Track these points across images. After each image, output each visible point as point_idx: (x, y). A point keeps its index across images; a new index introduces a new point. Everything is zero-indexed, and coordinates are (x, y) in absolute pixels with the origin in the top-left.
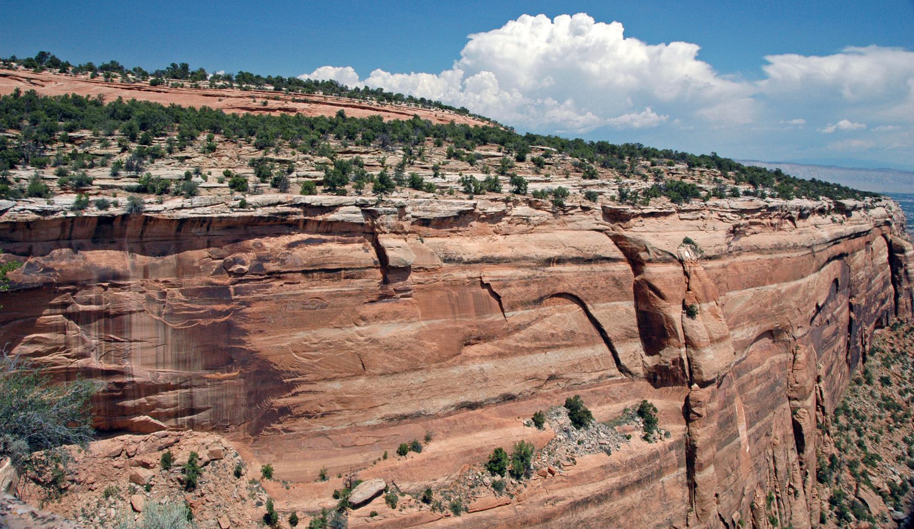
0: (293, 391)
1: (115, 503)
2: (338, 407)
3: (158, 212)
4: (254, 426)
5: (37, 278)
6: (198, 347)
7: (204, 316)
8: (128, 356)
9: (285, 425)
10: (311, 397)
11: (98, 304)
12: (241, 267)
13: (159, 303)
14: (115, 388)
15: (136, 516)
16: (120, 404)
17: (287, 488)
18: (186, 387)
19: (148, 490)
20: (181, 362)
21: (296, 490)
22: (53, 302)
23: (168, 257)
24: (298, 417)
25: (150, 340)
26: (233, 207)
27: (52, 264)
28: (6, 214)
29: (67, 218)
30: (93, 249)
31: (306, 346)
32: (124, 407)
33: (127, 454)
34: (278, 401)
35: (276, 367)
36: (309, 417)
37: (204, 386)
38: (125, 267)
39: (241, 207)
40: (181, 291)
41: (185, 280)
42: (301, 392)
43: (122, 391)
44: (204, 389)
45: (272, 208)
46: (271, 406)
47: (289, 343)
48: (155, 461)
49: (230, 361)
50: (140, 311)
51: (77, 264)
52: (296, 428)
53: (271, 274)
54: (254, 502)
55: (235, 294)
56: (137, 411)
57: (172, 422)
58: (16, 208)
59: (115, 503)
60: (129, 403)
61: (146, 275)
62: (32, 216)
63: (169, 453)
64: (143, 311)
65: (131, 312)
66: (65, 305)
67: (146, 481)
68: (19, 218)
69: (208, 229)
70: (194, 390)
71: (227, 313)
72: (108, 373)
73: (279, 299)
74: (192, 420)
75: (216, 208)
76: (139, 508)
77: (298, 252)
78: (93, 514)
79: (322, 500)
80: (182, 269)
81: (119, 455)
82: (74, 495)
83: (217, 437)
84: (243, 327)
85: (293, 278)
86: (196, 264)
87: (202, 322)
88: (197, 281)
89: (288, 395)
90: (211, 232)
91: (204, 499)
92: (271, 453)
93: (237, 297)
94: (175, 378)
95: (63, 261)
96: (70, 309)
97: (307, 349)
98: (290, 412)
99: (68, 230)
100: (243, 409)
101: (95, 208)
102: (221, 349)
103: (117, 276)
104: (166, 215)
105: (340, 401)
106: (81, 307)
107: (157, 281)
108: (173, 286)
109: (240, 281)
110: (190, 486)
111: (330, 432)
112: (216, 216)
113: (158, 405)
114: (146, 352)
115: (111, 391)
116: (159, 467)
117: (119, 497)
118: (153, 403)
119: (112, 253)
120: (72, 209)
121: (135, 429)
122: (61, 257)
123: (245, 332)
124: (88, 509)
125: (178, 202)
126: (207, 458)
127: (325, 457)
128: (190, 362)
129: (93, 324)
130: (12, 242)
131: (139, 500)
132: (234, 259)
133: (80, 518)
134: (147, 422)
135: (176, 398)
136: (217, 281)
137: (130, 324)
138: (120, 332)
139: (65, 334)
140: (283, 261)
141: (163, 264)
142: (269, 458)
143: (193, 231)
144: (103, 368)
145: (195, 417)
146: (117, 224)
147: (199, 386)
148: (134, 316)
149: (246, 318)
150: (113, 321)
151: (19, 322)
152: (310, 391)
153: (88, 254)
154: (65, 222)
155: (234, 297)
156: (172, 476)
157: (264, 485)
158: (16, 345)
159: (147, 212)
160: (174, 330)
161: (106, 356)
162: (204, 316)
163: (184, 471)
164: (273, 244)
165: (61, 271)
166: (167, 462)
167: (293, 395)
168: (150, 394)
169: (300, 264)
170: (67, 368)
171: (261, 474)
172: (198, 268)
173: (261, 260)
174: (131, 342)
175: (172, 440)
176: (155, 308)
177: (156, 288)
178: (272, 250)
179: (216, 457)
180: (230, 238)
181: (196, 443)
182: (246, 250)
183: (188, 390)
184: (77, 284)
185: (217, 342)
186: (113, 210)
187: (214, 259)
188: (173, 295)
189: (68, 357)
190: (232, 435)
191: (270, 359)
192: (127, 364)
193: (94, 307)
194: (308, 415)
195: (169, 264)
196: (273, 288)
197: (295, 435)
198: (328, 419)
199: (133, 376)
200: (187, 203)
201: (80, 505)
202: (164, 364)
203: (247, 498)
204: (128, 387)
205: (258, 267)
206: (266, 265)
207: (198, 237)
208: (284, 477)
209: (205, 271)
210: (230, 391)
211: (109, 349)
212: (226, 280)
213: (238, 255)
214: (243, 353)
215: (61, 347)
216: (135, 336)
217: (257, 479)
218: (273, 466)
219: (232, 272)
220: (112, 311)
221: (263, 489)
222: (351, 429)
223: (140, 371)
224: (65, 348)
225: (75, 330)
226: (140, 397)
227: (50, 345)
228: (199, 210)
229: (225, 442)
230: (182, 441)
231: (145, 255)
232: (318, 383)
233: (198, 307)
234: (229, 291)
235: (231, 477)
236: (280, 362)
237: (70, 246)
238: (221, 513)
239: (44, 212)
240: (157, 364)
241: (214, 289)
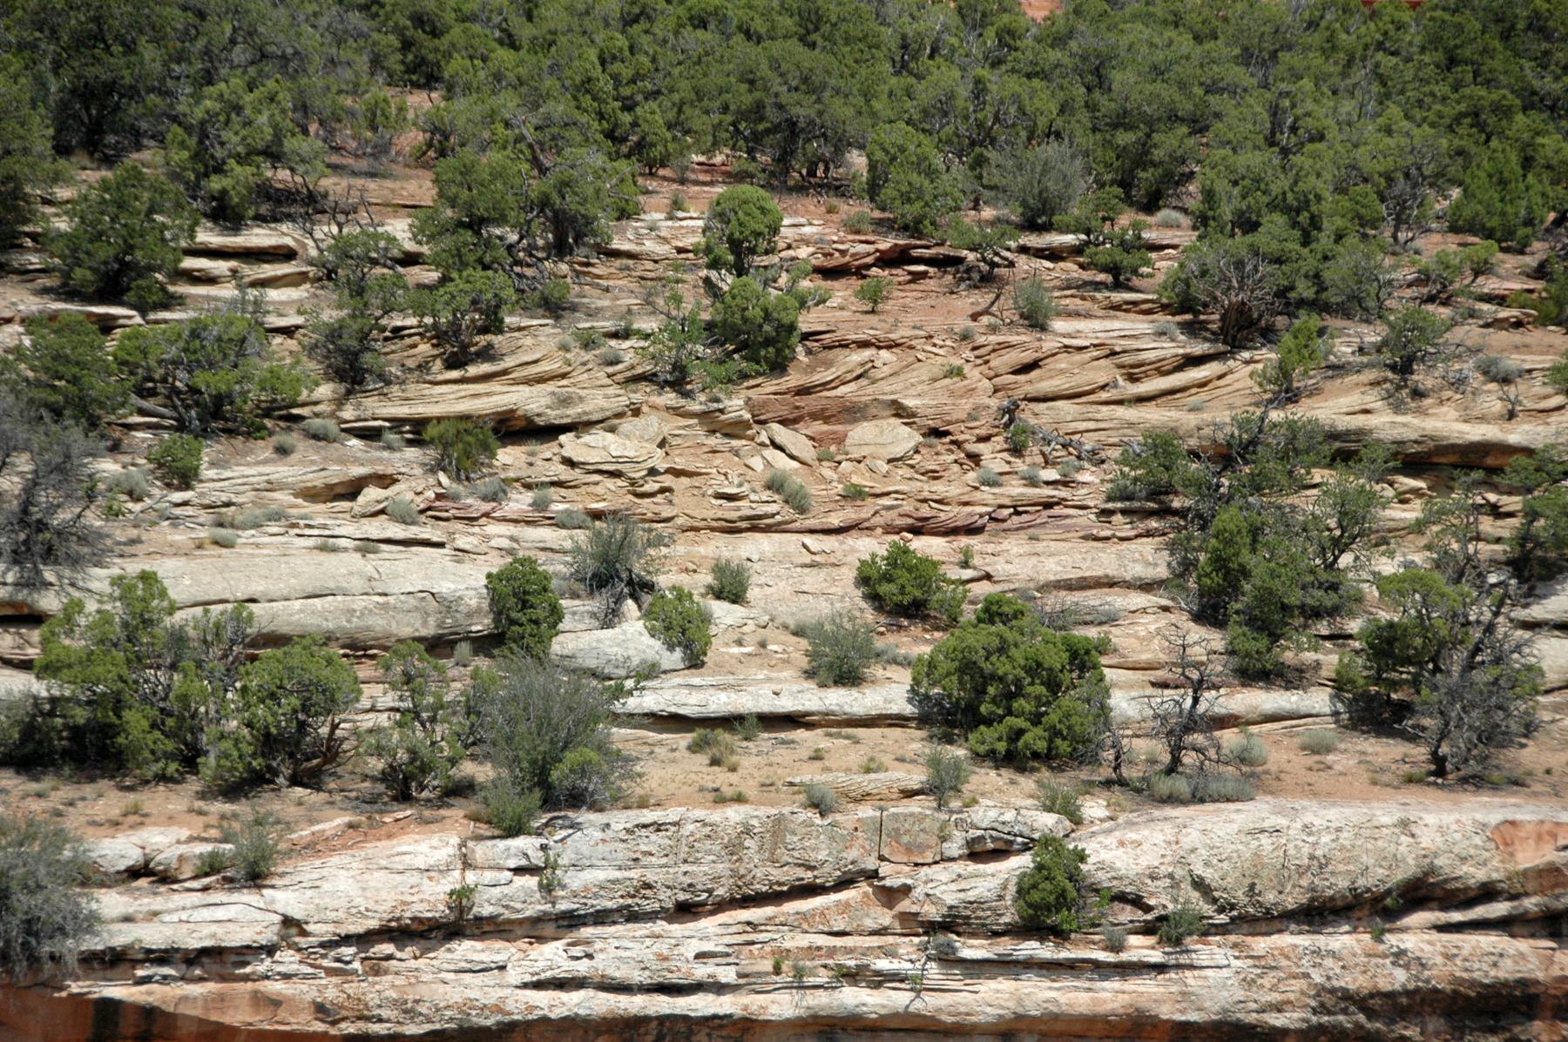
3: (215, 960)
26: (953, 923)
39: (1032, 926)
45: (1343, 940)
75: (794, 929)
112: (781, 1006)
125: (417, 862)
159: (115, 961)
228: (622, 950)
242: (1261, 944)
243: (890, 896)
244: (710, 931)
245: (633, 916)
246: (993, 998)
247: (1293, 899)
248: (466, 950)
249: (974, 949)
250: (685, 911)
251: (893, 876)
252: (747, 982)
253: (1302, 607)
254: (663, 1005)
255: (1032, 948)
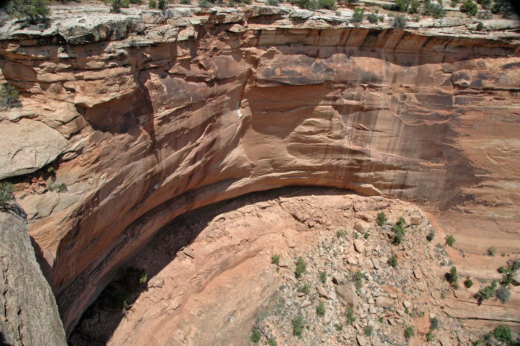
0: (480, 184)
1: (343, 242)
2: (510, 201)
3: (416, 28)
4: (444, 204)
5: (321, 76)
6: (419, 141)
7: (429, 118)
8: (369, 142)
9: (467, 208)
10: (492, 191)
11: (358, 100)
12: (465, 81)
13: (400, 104)
14: (355, 163)
15: (358, 256)
16: (356, 174)
17: (463, 256)
18: (404, 170)
19: (366, 238)
20: (405, 151)
21: (470, 259)
22: (328, 96)
23: (413, 68)
24: (478, 203)
25: (387, 131)
26: (472, 29)
27: (331, 65)
28: (307, 22)
29: (349, 28)
30: (360, 55)
31: (498, 151)
32: (357, 177)
33: (354, 209)
34: (467, 189)
35: (472, 164)
36: (486, 205)
37: (417, 170)
38: (381, 73)
39: (477, 30)
40: (417, 96)
41: (421, 87)
42: (485, 186)
43: (360, 166)
44: (416, 173)
45: (501, 32)
46: (461, 193)
47: (486, 147)
48: (372, 217)
49: (440, 155)
50: (385, 109)
51: (348, 67)
52: (474, 211)
53: (486, 89)
54: (439, 262)
55: (456, 103)
56: (365, 180)
57: (387, 191)
58: (314, 17)
59: (343, 242)
60: (362, 174)
61: (394, 81)
62: (325, 25)
63: (382, 214)
64: (388, 109)
65: (379, 109)
66: (335, 99)
67: (366, 231)
68: (317, 26)
69: (445, 47)
70: (409, 172)
71: (447, 117)
72: (354, 152)
73: (487, 111)
74: (401, 192)
75: (458, 29)
76: (360, 250)
77: (510, 73)
78: (329, 247)
79: (489, 271)
80: (421, 79)
81: (348, 209)
82: (318, 231)
83: (417, 208)
84: (456, 130)
85: (501, 95)
86: (431, 76)
87: (427, 122)
88: (429, 89)
89: (475, 186)
90: (447, 49)
91: (405, 253)
92: (452, 226)
93: (456, 105)
94: (398, 161)
95: (340, 64)
96: (338, 102)
97: (498, 153)
98: (473, 199)
99: (345, 38)
100: (440, 191)
101: (367, 21)
102: (436, 145)
103: (375, 80)
104: (421, 32)
105: (512, 197)
106: (346, 102)
107: (401, 86)
108: (412, 91)
109: (461, 93)
110: (396, 241)
111: (499, 219)
112: (457, 36)
113: (381, 178)
114: (382, 140)
115: (352, 164)
116: (374, 223)
117: (346, 239)
118: (377, 177)
119: (373, 60)
120: (351, 21)
121: (365, 193)
122: (338, 61)
123: (456, 134)
124: (325, 242)
125: (428, 21)
126: (409, 223)
127: (493, 237)
128: (411, 151)
129: (350, 115)
130: (306, 45)
131: (360, 244)
132: (461, 74)
133: (321, 249)
134: (370, 189)
135: (395, 176)
136: (444, 91)
137: (376, 118)
138: (368, 123)
139: (331, 120)
140: (498, 79)
141: (408, 73)
142: (451, 231)
143: (434, 47)
144: (352, 148)
145: (404, 191)
146: (381, 36)
147: (413, 170)
148: (380, 112)
149: (459, 123)
150: (364, 113)
151: (302, 108)
152: (492, 186)
153: (356, 59)
154: (347, 33)
155: (454, 106)
156: (384, 232)
157: (446, 250)
158: (298, 125)
159: (408, 28)
160: (406, 126)
161: (354, 140)
162: (429, 118)
163: (392, 230)
164: (493, 64)
165: (337, 72)
166: (381, 220)
167: (479, 187)
168: (378, 171)
169: (510, 84)
170: (327, 145)
171: (445, 241)
172: (432, 79)
173: (482, 77)
174: (373, 131)
175: (385, 204)
176: (396, 107)
177: (400, 92)
178: (491, 69)
179: (415, 223)
180: (460, 56)
181: (400, 210)
182: (471, 68)
183: (405, 172)
184: (346, 83)
185: (435, 140)
186: (380, 24)
187: (445, 72)
188: (411, 98)
189: (329, 137)
190: (426, 207)
191: (470, 158)
192: (367, 147)
193: (354, 102)
194: (485, 204)
195: (412, 73)
196: (484, 102)
197: (472, 217)
198: (499, 208)
199: (370, 157)
200: (437, 22)
201: (321, 239)
202: (393, 150)
203: (433, 257)
204: (364, 164)
205: (477, 84)
206: (484, 82)
207: (437, 52)
208: (461, 247)
209: (437, 81)
210: (434, 177)
211: (358, 134)
212: (451, 91)
213: (464, 71)
214: (451, 150)
215: (327, 129)
216: (378, 127)
217: (442, 244)
218: (455, 237)
219: (458, 85)
220: (366, 107)
221: (446, 253)
222: (515, 219)
223: (375, 153)
224: (329, 131)
225: (338, 118)
226: (370, 171)
227: (320, 128)
228: (446, 30)
229: (423, 214)
230: (392, 206)
231: (396, 64)
232: (500, 181)
233: (427, 110)
234: (452, 100)
235: (424, 239)
236: (476, 160)
237: (344, 52)
238: (416, 265)
239: (334, 22)
240: (388, 150)
241: (441, 97)
242: (495, 32)
243: (466, 26)
244: (452, 29)
245: (446, 27)
246: (474, 36)
247: (498, 29)
248: (433, 29)
249: (473, 32)
250: (450, 27)
251: (467, 25)
252: (455, 33)
253: (380, 7)
254: (448, 35)
255: (477, 32)
